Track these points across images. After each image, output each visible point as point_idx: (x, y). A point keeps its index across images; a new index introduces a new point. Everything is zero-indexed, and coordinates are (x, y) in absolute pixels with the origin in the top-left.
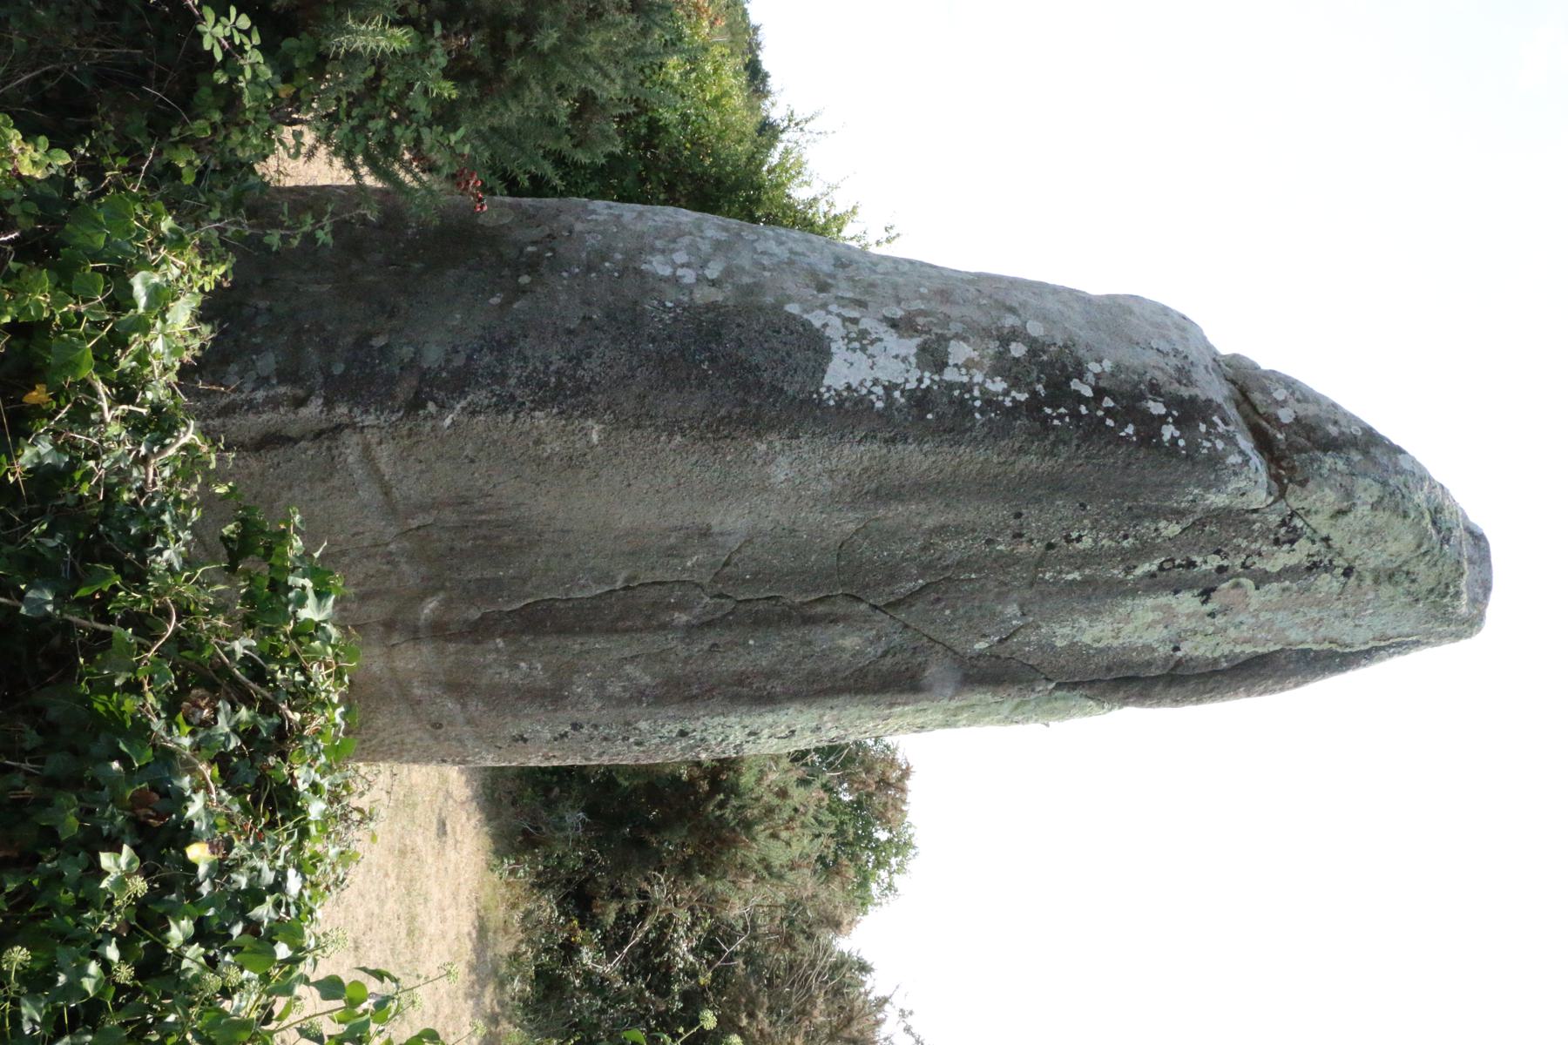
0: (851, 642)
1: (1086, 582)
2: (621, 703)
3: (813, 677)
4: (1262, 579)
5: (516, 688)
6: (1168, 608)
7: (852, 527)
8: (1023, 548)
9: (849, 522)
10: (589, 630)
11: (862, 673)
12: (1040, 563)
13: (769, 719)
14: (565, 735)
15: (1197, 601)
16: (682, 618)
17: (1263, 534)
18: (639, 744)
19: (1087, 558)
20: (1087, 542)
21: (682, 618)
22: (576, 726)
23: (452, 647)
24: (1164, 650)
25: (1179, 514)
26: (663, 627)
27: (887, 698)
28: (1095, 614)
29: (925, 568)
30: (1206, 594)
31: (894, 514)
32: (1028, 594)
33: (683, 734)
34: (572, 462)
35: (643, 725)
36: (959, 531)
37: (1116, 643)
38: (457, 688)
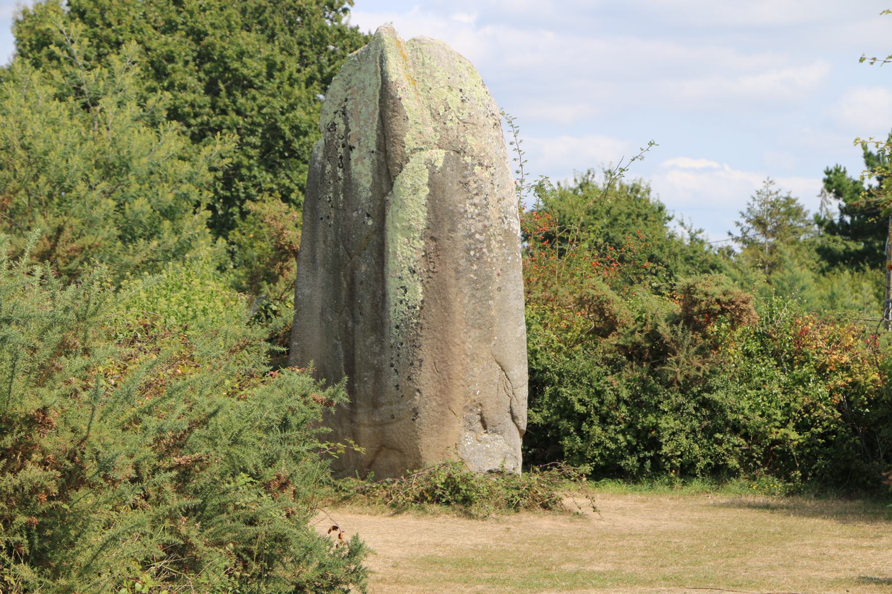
0: (363, 268)
1: (344, 191)
2: (382, 348)
3: (376, 280)
4: (348, 130)
5: (374, 383)
6: (356, 161)
7: (322, 270)
8: (333, 215)
9: (321, 270)
10: (353, 355)
11: (377, 263)
12: (337, 209)
13: (391, 296)
14: (396, 371)
15: (354, 151)
16: (350, 324)
17: (333, 135)
18: (402, 344)
19: (336, 194)
20: (331, 195)
21: (350, 324)
22: (392, 365)
23: (358, 402)
24: (374, 156)
25: (324, 167)
26: (353, 330)
27: (385, 254)
28: (357, 185)
29: (337, 246)
30: (351, 148)
31: (319, 257)
32: (348, 210)
33: (397, 327)
34: (303, 352)
35: (392, 341)
36: (326, 237)
37: (370, 174)
38: (375, 405)
